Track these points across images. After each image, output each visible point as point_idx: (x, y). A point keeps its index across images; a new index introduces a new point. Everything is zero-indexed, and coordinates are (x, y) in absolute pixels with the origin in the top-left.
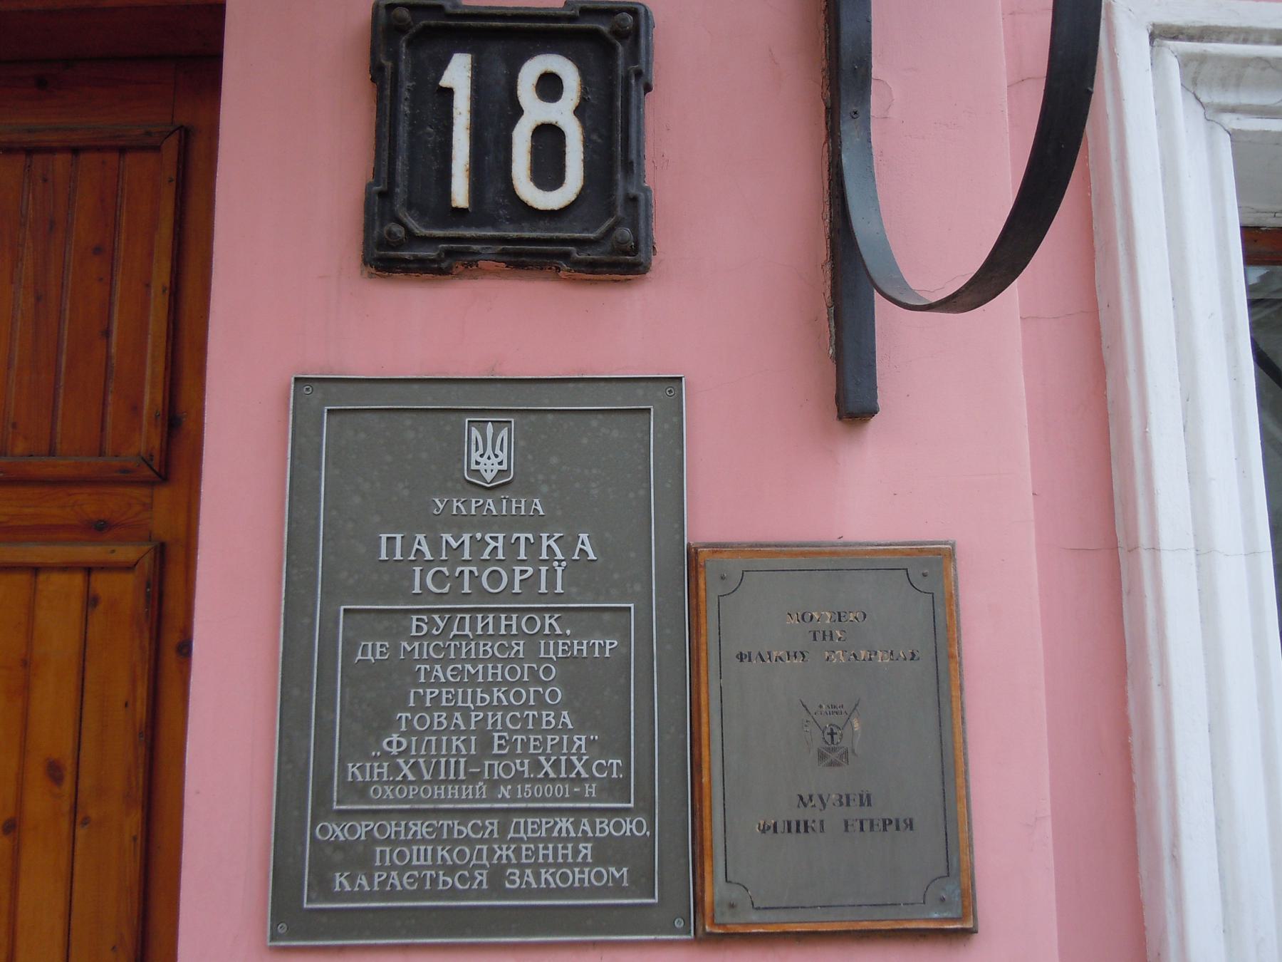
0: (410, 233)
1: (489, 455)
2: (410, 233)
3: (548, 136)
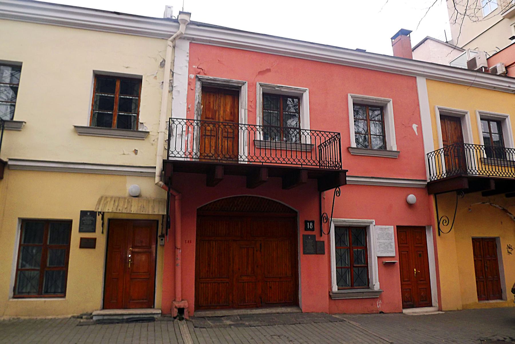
0: (306, 229)
2: (306, 229)
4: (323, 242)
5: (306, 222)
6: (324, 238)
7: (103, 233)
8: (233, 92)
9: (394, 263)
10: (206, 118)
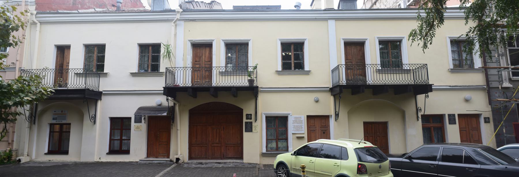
0: (247, 119)
2: (247, 119)
5: (247, 115)
8: (209, 46)
9: (303, 137)
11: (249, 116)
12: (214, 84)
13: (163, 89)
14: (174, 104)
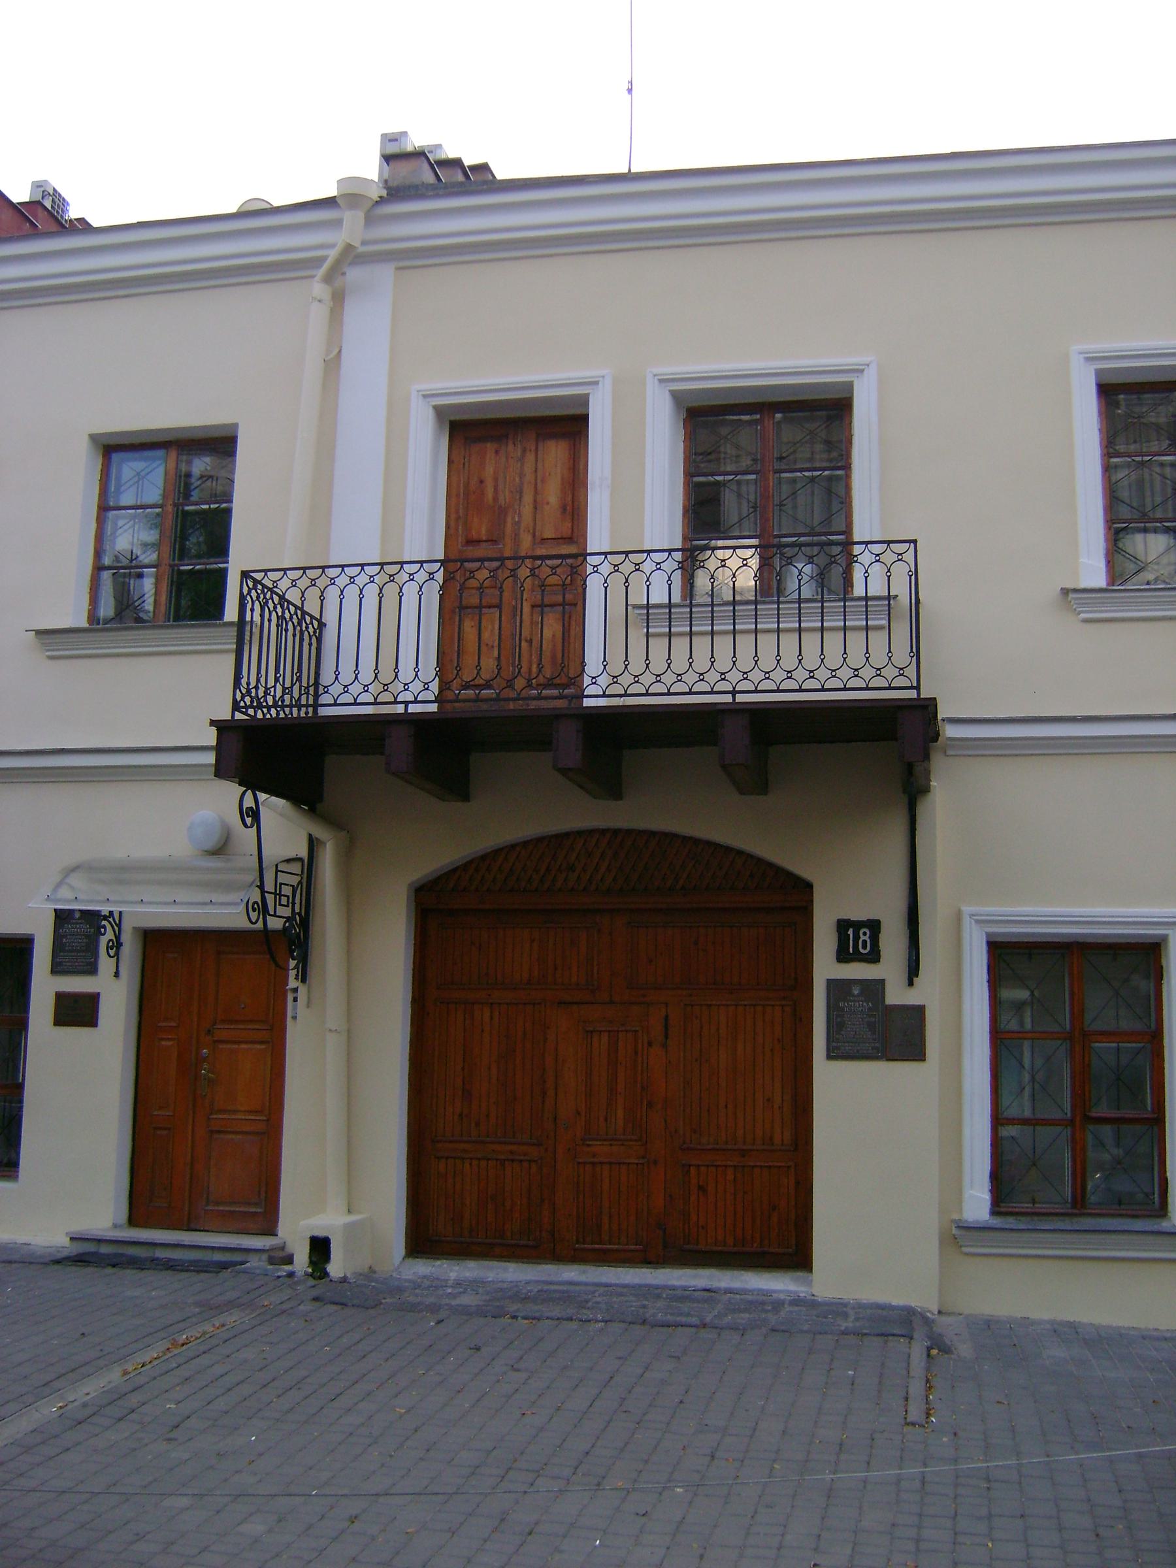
0: (844, 955)
1: (856, 992)
2: (844, 955)
3: (865, 942)
4: (920, 1011)
5: (843, 926)
6: (926, 993)
7: (117, 975)
10: (470, 542)
11: (858, 939)
12: (597, 693)
13: (210, 737)
14: (313, 844)
